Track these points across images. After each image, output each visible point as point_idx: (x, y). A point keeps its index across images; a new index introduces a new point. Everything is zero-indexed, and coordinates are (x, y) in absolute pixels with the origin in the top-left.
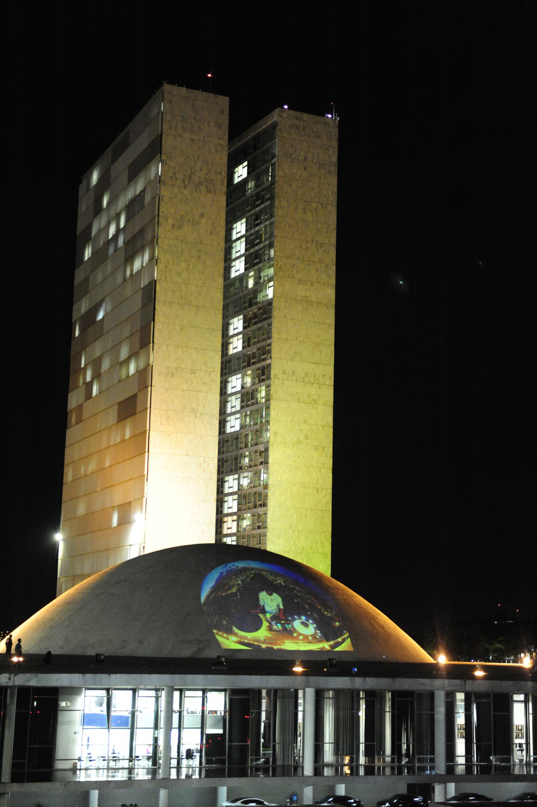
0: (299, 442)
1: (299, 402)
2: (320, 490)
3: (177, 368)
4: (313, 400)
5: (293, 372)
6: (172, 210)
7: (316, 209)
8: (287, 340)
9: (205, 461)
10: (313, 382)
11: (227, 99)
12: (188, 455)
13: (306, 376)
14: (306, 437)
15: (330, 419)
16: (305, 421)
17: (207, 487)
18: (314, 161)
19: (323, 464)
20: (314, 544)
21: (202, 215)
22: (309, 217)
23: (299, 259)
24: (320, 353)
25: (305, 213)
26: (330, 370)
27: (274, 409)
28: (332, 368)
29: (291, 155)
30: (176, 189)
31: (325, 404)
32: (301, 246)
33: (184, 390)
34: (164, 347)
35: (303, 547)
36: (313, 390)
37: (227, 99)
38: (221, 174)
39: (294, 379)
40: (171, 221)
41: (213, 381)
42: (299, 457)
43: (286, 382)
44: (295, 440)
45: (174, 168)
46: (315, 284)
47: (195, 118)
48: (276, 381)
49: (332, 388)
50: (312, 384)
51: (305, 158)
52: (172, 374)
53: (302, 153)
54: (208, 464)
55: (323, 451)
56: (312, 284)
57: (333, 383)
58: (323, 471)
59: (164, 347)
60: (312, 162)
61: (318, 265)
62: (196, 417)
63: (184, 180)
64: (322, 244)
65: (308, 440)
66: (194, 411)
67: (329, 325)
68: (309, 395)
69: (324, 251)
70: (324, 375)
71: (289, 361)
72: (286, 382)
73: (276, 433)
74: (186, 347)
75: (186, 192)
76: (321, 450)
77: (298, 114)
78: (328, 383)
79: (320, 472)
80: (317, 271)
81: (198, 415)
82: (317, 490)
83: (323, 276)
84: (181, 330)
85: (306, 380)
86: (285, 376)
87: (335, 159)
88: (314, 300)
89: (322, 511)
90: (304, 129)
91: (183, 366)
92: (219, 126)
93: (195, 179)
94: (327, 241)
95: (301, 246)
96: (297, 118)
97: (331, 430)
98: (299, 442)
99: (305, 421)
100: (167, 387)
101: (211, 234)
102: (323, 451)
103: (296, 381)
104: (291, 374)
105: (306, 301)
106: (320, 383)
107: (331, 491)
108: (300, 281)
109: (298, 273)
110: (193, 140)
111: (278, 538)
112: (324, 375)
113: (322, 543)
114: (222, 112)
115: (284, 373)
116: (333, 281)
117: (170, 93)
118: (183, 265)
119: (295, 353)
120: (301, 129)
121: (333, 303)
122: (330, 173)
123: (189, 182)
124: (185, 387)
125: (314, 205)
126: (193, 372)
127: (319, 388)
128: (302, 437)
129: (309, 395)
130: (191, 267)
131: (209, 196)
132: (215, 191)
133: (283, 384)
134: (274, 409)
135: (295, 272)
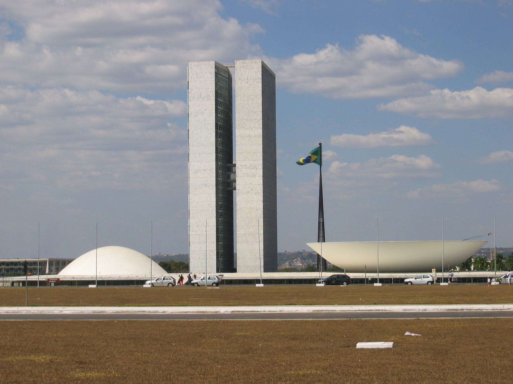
0: (249, 192)
8: (242, 153)
14: (252, 190)
21: (206, 110)
31: (259, 176)
56: (252, 129)
59: (193, 163)
68: (252, 173)
73: (239, 190)
77: (244, 61)
87: (260, 76)
93: (202, 96)
94: (258, 110)
96: (243, 63)
98: (249, 192)
108: (246, 129)
115: (241, 166)
118: (199, 130)
125: (252, 97)
129: (252, 173)
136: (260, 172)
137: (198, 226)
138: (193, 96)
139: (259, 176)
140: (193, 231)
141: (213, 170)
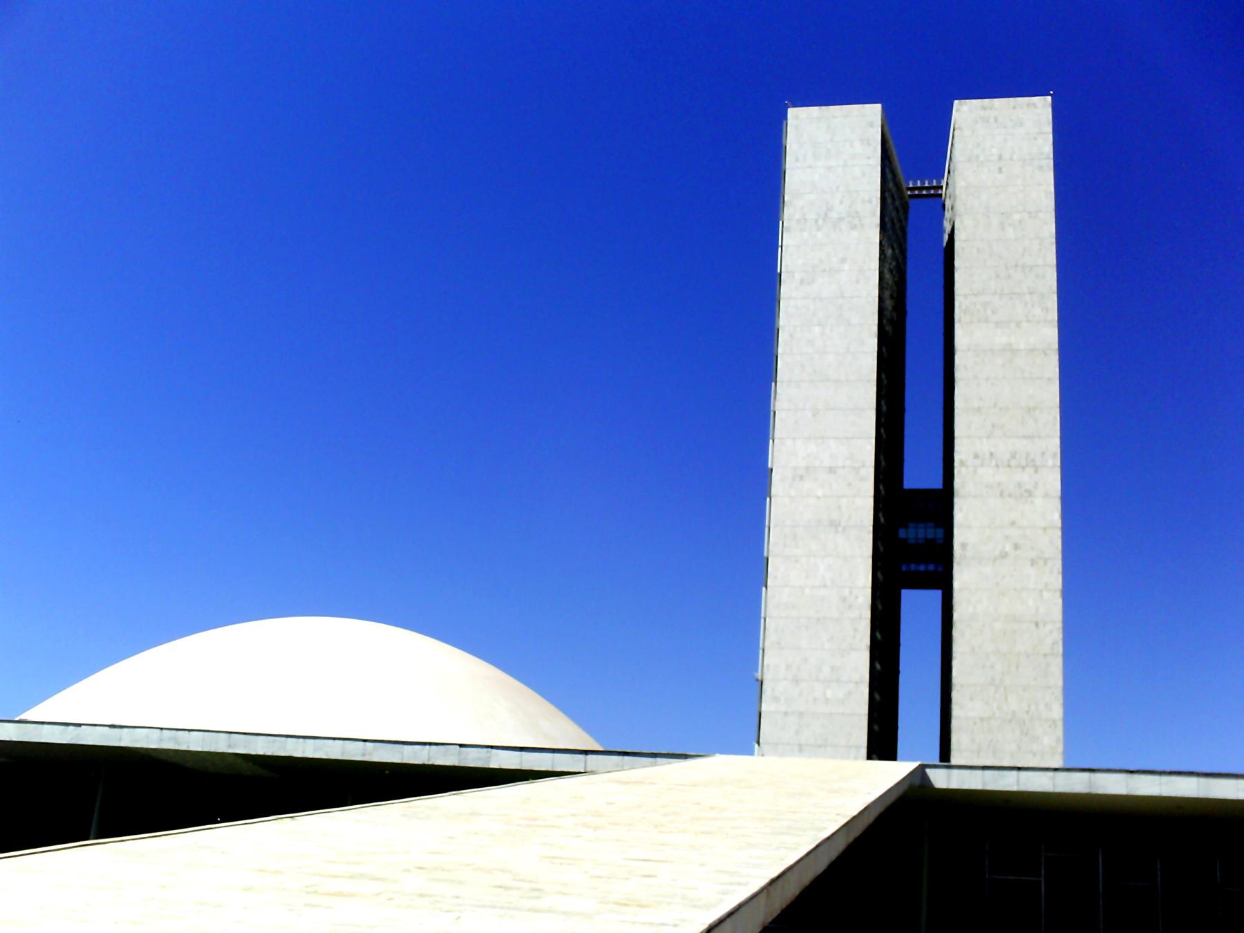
1: (1001, 495)
2: (1041, 625)
3: (807, 468)
4: (1026, 491)
5: (991, 454)
6: (800, 262)
7: (1020, 222)
8: (979, 409)
9: (851, 593)
10: (1024, 463)
11: (878, 107)
12: (825, 586)
13: (1013, 456)
14: (1016, 547)
15: (1056, 517)
16: (1013, 523)
17: (855, 630)
18: (1015, 157)
19: (1046, 584)
20: (1033, 708)
21: (843, 260)
22: (1010, 233)
23: (995, 294)
24: (1036, 421)
25: (1003, 229)
26: (1054, 444)
27: (961, 510)
28: (1058, 441)
29: (977, 157)
30: (805, 234)
31: (1046, 496)
32: (998, 276)
33: (818, 498)
34: (789, 442)
35: (1014, 712)
36: (1026, 477)
37: (878, 107)
38: (870, 202)
39: (994, 463)
40: (797, 276)
41: (862, 479)
42: (1004, 577)
43: (980, 471)
44: (997, 552)
45: (802, 208)
46: (1025, 325)
47: (832, 140)
48: (963, 470)
49: (1058, 470)
50: (1023, 468)
51: (1000, 158)
52: (801, 478)
53: (994, 150)
54: (856, 597)
55: (1045, 563)
56: (1018, 324)
57: (1058, 463)
58: (1046, 595)
59: (789, 442)
60: (1011, 159)
61: (1028, 298)
62: (837, 532)
63: (816, 221)
64: (1032, 268)
65: (1018, 552)
66: (834, 525)
67: (1049, 379)
69: (1037, 276)
70: (1043, 454)
71: (985, 441)
72: (980, 471)
73: (964, 546)
74: (822, 438)
75: (819, 235)
76: (1041, 563)
77: (986, 101)
78: (1050, 463)
79: (1041, 596)
80: (1026, 304)
81: (840, 529)
82: (1037, 624)
83: (1037, 311)
84: (814, 415)
85: (1013, 463)
86: (978, 462)
88: (1022, 347)
89: (1045, 655)
90: (996, 120)
91: (817, 464)
92: (865, 141)
93: (834, 215)
94: (1040, 261)
95: (998, 276)
96: (984, 108)
97: (1059, 533)
98: (1004, 555)
99: (1013, 523)
100: (793, 493)
101: (857, 282)
102: (1045, 563)
103: (997, 466)
104: (988, 456)
105: (1010, 350)
106: (1038, 463)
107: (1060, 625)
108: (998, 324)
109: (994, 312)
110: (829, 168)
111: (972, 699)
112: (1043, 454)
113: (1046, 705)
114: (871, 125)
115: (976, 456)
116: (1054, 315)
117: (797, 118)
118: (817, 329)
119: (993, 426)
120: (992, 120)
121: (1056, 346)
122: (1041, 168)
123: (824, 220)
124: (820, 493)
125: (1017, 217)
126: (832, 470)
127: (1036, 472)
128: (1008, 548)
129: (1019, 485)
130: (828, 330)
131: (855, 233)
132: (862, 226)
133: (975, 472)
134: (961, 510)
135: (989, 312)
136: (1053, 480)
137: (796, 681)
138: (797, 216)
139: (1046, 496)
140: (776, 699)
141: (863, 472)
